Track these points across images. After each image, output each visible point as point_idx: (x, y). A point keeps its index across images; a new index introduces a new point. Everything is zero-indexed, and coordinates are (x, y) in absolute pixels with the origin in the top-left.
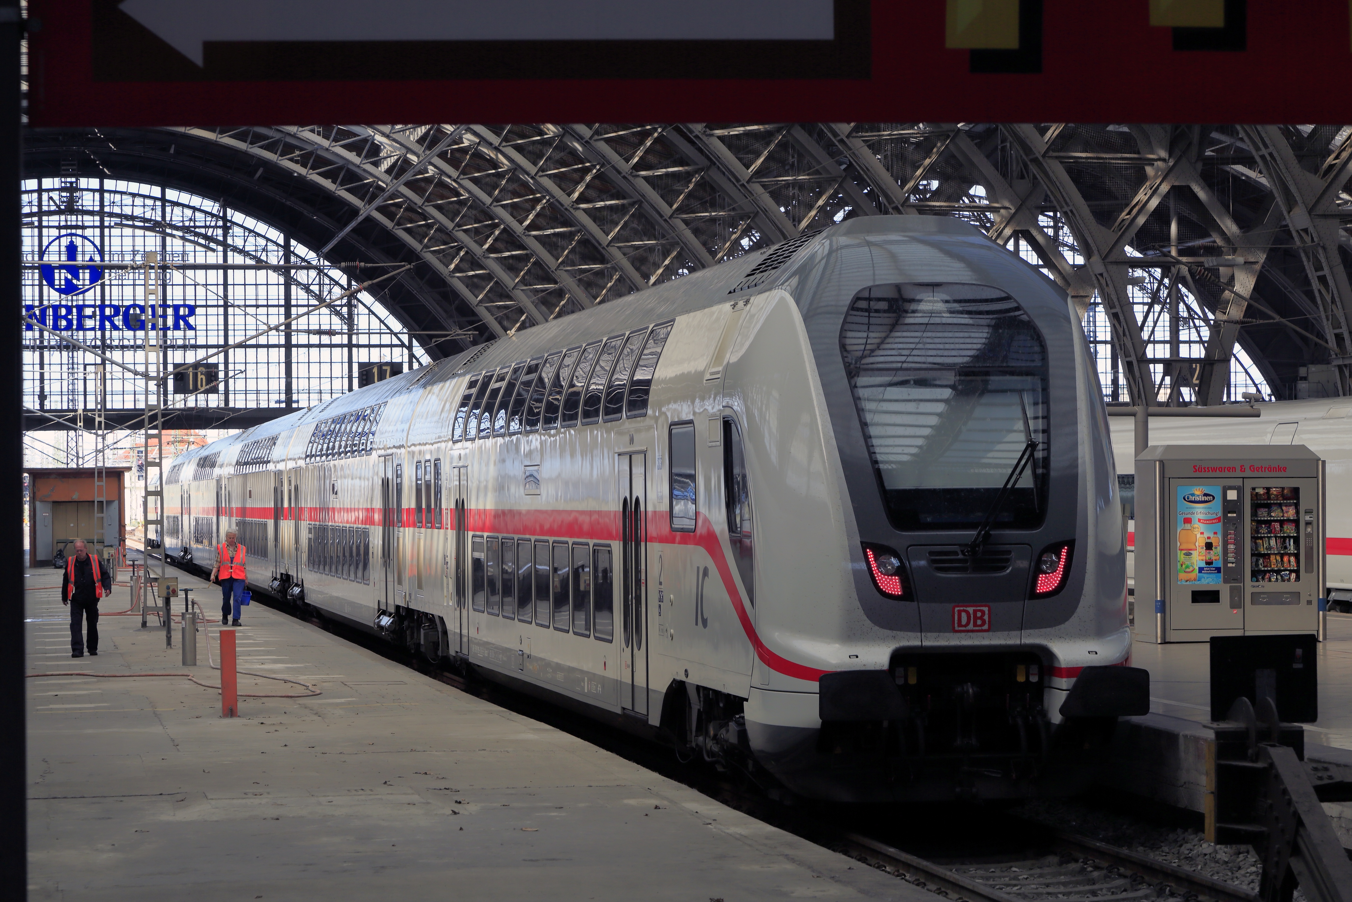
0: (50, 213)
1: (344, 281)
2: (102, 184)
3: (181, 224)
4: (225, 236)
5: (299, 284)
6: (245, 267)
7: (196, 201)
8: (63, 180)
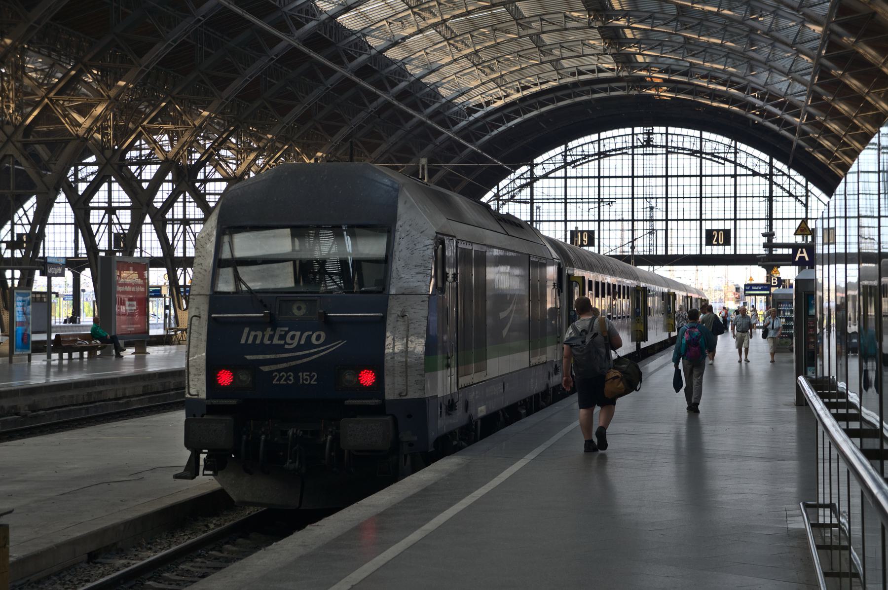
0: (637, 147)
1: (803, 182)
2: (667, 130)
3: (711, 152)
4: (736, 157)
5: (776, 184)
6: (746, 175)
7: (720, 138)
8: (645, 128)
